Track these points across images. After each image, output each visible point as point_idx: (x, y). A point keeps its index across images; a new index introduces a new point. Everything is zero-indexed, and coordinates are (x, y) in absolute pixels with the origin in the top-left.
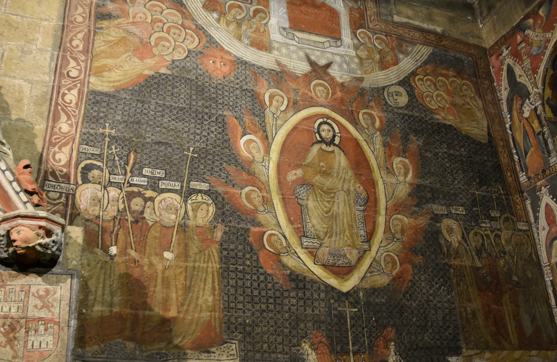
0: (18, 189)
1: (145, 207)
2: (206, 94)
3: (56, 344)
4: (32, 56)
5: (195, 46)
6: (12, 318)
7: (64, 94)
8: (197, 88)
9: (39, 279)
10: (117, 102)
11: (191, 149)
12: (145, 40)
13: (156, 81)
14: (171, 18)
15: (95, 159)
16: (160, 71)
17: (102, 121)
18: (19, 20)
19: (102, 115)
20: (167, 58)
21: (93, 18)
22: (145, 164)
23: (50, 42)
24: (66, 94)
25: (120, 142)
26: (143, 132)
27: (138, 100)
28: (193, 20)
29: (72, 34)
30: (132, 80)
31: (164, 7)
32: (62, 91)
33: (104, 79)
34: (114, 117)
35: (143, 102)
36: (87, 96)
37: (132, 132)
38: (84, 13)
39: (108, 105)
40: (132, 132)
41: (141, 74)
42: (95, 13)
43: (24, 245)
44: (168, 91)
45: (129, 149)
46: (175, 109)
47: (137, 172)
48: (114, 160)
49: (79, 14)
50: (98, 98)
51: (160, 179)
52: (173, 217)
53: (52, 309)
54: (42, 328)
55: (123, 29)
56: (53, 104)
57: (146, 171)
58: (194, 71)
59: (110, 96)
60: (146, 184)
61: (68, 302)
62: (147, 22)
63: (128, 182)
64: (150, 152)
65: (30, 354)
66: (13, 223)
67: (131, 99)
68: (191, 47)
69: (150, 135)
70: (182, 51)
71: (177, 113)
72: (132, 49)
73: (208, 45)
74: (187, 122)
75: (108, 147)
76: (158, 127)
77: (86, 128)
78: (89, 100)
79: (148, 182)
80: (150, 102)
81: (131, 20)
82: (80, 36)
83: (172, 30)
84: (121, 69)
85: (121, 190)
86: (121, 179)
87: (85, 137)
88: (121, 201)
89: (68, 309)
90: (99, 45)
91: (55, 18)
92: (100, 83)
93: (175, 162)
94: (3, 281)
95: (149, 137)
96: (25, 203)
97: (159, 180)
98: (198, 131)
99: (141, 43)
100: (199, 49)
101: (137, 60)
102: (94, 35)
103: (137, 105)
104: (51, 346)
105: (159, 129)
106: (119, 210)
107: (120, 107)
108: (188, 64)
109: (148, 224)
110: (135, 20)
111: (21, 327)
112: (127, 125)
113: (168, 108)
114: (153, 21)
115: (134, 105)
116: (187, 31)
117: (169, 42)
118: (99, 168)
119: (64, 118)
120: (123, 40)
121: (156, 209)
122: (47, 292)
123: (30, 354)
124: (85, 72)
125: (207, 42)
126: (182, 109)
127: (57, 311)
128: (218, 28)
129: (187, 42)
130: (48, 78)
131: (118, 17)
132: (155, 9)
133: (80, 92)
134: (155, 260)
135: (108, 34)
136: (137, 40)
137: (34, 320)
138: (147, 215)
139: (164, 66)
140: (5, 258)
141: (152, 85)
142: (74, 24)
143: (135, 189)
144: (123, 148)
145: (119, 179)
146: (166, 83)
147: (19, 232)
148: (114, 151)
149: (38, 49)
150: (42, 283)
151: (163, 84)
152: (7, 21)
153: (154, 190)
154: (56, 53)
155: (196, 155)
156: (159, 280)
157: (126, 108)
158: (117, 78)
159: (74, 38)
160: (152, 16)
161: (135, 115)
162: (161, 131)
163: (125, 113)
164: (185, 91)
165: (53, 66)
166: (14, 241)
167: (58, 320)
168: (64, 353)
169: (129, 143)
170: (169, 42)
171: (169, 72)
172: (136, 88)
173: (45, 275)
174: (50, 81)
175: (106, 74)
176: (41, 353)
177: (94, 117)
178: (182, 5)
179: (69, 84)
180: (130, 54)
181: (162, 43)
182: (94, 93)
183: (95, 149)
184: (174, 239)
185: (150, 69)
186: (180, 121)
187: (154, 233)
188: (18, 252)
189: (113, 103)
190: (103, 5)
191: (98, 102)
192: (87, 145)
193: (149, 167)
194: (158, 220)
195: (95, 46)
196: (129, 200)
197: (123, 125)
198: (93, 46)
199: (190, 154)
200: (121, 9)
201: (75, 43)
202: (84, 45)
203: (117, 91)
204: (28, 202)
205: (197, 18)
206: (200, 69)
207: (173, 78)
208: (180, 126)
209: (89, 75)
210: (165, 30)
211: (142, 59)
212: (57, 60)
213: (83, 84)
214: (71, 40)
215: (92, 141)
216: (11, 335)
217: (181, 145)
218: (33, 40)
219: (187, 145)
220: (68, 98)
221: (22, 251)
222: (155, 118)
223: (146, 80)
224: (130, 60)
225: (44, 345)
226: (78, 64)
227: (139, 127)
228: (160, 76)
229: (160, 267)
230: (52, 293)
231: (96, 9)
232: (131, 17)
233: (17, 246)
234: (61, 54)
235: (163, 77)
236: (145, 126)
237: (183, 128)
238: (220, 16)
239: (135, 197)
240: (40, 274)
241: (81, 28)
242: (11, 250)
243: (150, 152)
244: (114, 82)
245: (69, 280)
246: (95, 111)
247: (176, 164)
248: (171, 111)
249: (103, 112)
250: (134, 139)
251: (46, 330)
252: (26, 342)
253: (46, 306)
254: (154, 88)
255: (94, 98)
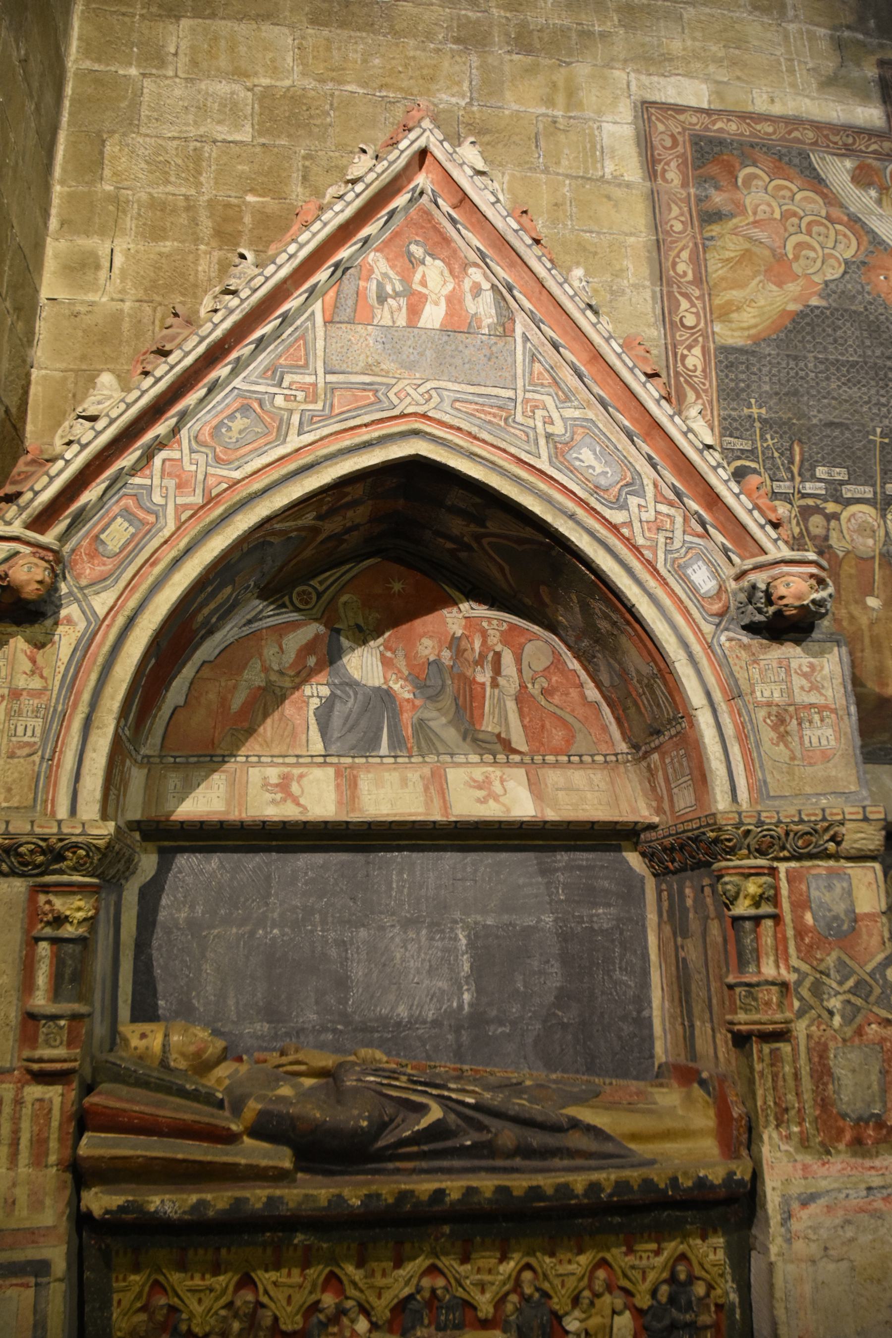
0: (763, 521)
1: (828, 530)
2: (885, 336)
3: (837, 740)
4: (627, 297)
5: (853, 253)
6: (777, 705)
7: (684, 357)
8: (869, 327)
9: (798, 649)
10: (759, 361)
11: (879, 430)
12: (779, 251)
13: (808, 320)
14: (809, 207)
15: (747, 458)
16: (810, 303)
17: (744, 395)
18: (596, 240)
19: (742, 385)
20: (817, 279)
21: (696, 223)
22: (817, 461)
23: (645, 271)
24: (687, 356)
25: (775, 428)
26: (805, 408)
27: (788, 356)
28: (842, 206)
29: (673, 254)
30: (773, 323)
31: (795, 189)
32: (679, 352)
33: (733, 326)
34: (760, 387)
35: (795, 358)
36: (716, 357)
37: (789, 409)
38: (682, 214)
39: (747, 368)
40: (789, 409)
41: (784, 310)
42: (699, 212)
43: (797, 603)
44: (829, 335)
45: (791, 439)
46: (844, 366)
47: (808, 474)
48: (773, 457)
49: (676, 218)
50: (732, 358)
51: (842, 483)
52: (870, 542)
53: (823, 691)
54: (816, 718)
55: (743, 236)
56: (672, 374)
57: (821, 472)
58: (860, 297)
59: (747, 352)
60: (823, 492)
61: (840, 680)
62: (775, 219)
63: (799, 492)
64: (821, 440)
65: (810, 754)
66: (776, 571)
67: (778, 355)
68: (848, 255)
69: (815, 413)
70: (836, 264)
71: (848, 371)
72: (763, 268)
73: (871, 248)
74: (864, 386)
75: (762, 436)
76: (825, 398)
77: (725, 409)
78: (721, 362)
79: (826, 489)
80: (805, 357)
81: (751, 219)
82: (685, 255)
83: (815, 229)
84: (754, 305)
85: (791, 503)
86: (789, 488)
87: (726, 424)
88: (794, 522)
89: (842, 690)
90: (715, 267)
91: (643, 229)
92: (729, 333)
93: (859, 453)
94: (754, 654)
95: (815, 416)
96: (776, 541)
97: (841, 485)
98: (883, 400)
99: (774, 256)
100: (861, 257)
101: (774, 288)
102: (705, 252)
103: (788, 364)
104: (833, 743)
105: (825, 401)
106: (794, 537)
107: (765, 370)
108: (849, 286)
109: (837, 556)
110: (758, 218)
111: (791, 718)
112: (780, 399)
113: (833, 364)
114: (786, 215)
115: (784, 365)
116: (838, 227)
117: (814, 250)
118: (755, 471)
119: (691, 396)
120: (746, 256)
121: (845, 532)
122: (812, 666)
123: (810, 754)
124: (705, 317)
125: (870, 243)
126: (853, 365)
127: (829, 693)
128: (881, 215)
129: (840, 247)
130: (653, 333)
131: (732, 216)
132: (782, 193)
133: (705, 351)
134: (856, 611)
135: (723, 248)
136: (767, 253)
137: (805, 707)
138: (834, 542)
139: (814, 293)
140: (760, 622)
141: (803, 328)
142: (671, 236)
143: (810, 502)
144: (781, 437)
145: (784, 487)
146: (823, 322)
147: (788, 585)
148: (770, 442)
149: (632, 285)
150: (803, 655)
151: (818, 325)
152: (579, 244)
153: (836, 501)
154: (658, 289)
155: (887, 441)
156: (867, 641)
157: (774, 371)
158: (753, 321)
159: (677, 260)
160: (780, 206)
161: (788, 381)
162: (830, 404)
163: (775, 379)
164: (853, 333)
165: (658, 311)
166: (782, 598)
167: (833, 706)
168: (851, 751)
169: (790, 429)
170: (814, 249)
171: (824, 303)
172: (782, 335)
173: (804, 644)
174: (660, 337)
175: (734, 316)
176: (823, 752)
177: (732, 390)
178: (821, 180)
179: (687, 339)
180: (761, 277)
181: (804, 252)
182: (725, 350)
183: (744, 442)
184: (877, 577)
185: (795, 300)
186: (855, 385)
187: (848, 569)
188: (788, 613)
189: (753, 365)
190: (707, 197)
191: (732, 364)
192: (731, 436)
193: (824, 466)
194: (850, 548)
195: (709, 270)
196: (806, 520)
197: (775, 400)
198: (706, 271)
199: (878, 440)
200: (733, 201)
201: (681, 267)
202: (693, 270)
203: (756, 344)
204: (778, 539)
205: (846, 201)
206: (869, 293)
207: (832, 314)
208: (855, 392)
209: (712, 321)
210: (804, 230)
211: (780, 285)
212: (662, 301)
213: (706, 337)
214: (674, 264)
215: (737, 429)
216: (782, 729)
217: (863, 426)
218: (622, 270)
219: (872, 425)
220: (690, 362)
221: (794, 612)
222: (818, 384)
223: (793, 321)
224: (763, 288)
225: (824, 742)
226: (693, 305)
227: (798, 401)
228: (812, 311)
229: (864, 621)
230: (818, 668)
231: (698, 205)
232: (750, 212)
233: (786, 606)
234: (665, 289)
235: (817, 312)
236: (805, 398)
237: (860, 397)
238: (881, 194)
239: (812, 514)
240: (798, 642)
241: (684, 242)
242: (771, 610)
243: (821, 440)
244: (748, 328)
245: (836, 649)
246: (732, 380)
247: (860, 458)
248: (838, 370)
249: (743, 381)
250: (794, 421)
251: (822, 720)
252: (801, 738)
253: (815, 687)
254: (808, 333)
255: (726, 358)
